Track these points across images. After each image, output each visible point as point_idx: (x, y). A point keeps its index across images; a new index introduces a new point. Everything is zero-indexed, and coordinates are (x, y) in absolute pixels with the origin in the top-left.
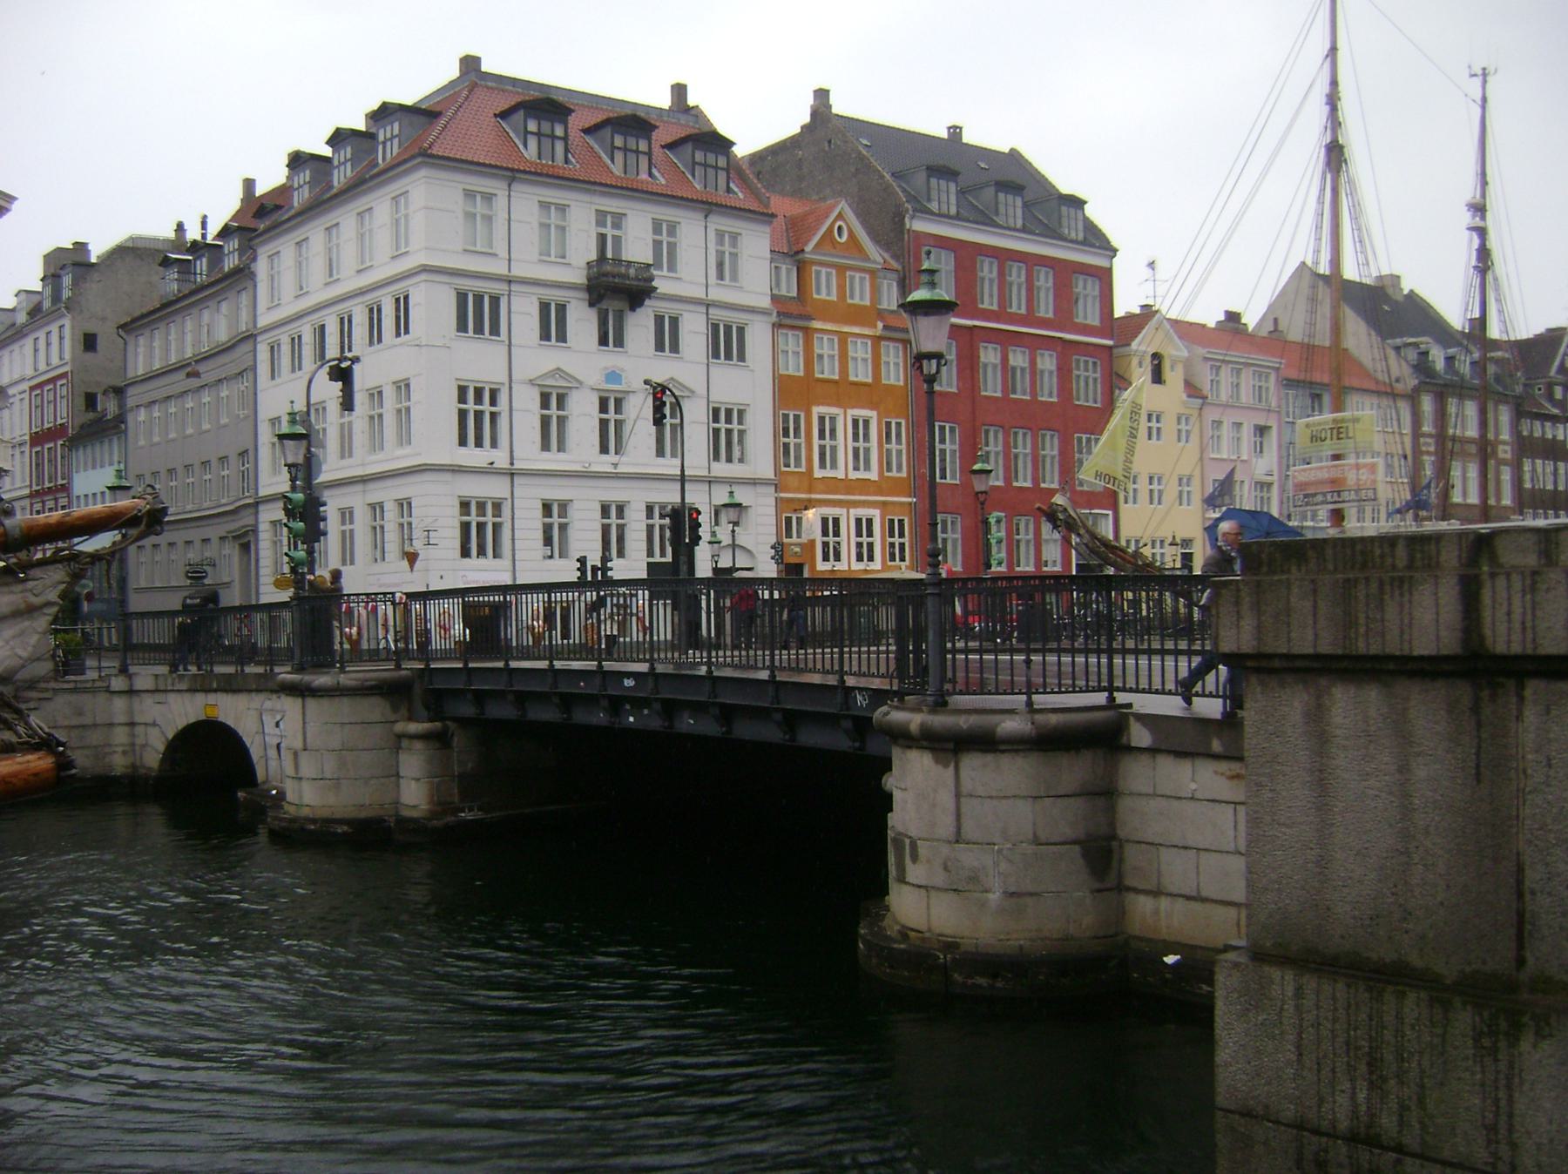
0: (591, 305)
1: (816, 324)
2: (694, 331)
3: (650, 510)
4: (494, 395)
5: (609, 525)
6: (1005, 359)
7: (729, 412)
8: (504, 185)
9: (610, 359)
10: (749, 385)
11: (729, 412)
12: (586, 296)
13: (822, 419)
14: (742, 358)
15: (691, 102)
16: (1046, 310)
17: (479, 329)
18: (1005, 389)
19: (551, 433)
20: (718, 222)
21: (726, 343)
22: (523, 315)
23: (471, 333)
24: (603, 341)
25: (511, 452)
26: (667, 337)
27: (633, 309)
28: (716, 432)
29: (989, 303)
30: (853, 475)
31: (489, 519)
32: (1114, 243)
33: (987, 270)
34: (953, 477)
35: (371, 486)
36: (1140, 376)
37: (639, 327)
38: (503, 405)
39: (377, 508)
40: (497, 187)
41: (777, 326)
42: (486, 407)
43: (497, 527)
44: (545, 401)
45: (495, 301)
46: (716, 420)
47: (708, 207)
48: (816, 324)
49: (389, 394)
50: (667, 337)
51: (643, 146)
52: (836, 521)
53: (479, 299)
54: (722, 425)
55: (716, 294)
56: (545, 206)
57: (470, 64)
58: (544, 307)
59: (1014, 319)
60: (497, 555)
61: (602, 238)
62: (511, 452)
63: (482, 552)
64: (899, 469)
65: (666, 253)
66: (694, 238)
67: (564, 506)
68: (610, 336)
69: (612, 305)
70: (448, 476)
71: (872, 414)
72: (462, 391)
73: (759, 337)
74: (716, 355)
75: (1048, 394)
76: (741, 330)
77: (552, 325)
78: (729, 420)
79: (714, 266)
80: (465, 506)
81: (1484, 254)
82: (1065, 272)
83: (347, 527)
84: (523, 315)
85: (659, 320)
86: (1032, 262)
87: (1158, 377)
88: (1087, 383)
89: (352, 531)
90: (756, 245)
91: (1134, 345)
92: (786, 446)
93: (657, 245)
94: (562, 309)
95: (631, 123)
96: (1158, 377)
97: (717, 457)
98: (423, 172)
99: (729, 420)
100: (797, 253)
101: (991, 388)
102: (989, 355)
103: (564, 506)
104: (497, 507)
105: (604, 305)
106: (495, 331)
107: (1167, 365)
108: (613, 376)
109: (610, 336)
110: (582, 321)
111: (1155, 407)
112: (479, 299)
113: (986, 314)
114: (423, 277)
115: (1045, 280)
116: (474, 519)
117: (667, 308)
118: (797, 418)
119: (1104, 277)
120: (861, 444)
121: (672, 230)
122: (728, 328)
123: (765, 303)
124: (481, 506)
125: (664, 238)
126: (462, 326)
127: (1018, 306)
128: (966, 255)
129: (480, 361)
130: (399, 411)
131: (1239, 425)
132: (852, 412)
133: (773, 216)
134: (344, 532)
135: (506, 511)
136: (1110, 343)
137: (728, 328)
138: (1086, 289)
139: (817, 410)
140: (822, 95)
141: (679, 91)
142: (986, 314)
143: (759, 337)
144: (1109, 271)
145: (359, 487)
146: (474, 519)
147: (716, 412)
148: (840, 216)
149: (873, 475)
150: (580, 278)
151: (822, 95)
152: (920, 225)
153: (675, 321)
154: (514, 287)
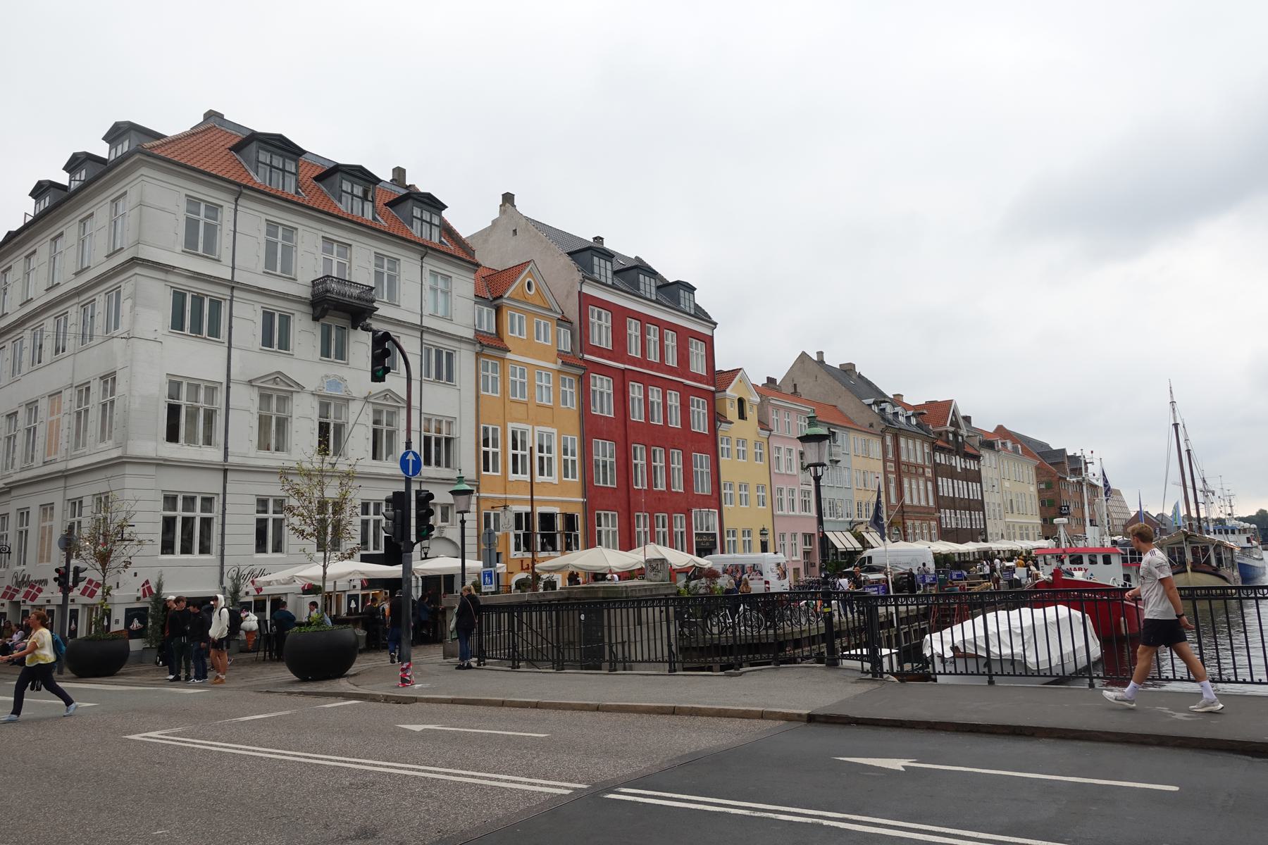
0: (315, 319)
3: (365, 507)
5: (266, 520)
6: (646, 396)
8: (231, 198)
9: (333, 369)
12: (310, 310)
13: (514, 434)
15: (408, 183)
16: (672, 361)
18: (646, 418)
19: (273, 431)
20: (431, 264)
22: (246, 320)
23: (187, 331)
24: (326, 352)
25: (226, 448)
26: (383, 355)
27: (355, 328)
29: (635, 352)
31: (198, 514)
32: (714, 319)
33: (633, 328)
34: (612, 483)
35: (72, 482)
39: (77, 504)
43: (206, 523)
45: (216, 304)
49: (96, 387)
53: (198, 300)
55: (428, 322)
58: (268, 317)
59: (651, 365)
60: (205, 549)
61: (328, 262)
62: (226, 448)
63: (187, 549)
64: (574, 476)
68: (333, 349)
69: (334, 321)
70: (151, 470)
71: (555, 431)
73: (465, 361)
75: (675, 422)
76: (450, 356)
77: (275, 334)
80: (170, 501)
82: (684, 336)
83: (47, 524)
84: (246, 320)
86: (662, 325)
87: (742, 416)
89: (51, 528)
91: (728, 391)
92: (486, 454)
93: (379, 275)
94: (286, 320)
96: (742, 416)
98: (144, 170)
100: (495, 299)
101: (637, 415)
102: (636, 391)
104: (208, 502)
105: (327, 320)
106: (214, 332)
107: (747, 406)
109: (333, 349)
110: (305, 334)
112: (198, 300)
113: (633, 361)
114: (137, 270)
115: (671, 340)
116: (179, 514)
119: (709, 342)
124: (189, 501)
126: (177, 324)
127: (653, 357)
128: (620, 316)
129: (198, 359)
130: (104, 405)
131: (790, 451)
132: (537, 428)
133: (478, 265)
134: (44, 528)
135: (217, 506)
136: (713, 388)
138: (697, 350)
140: (508, 198)
142: (633, 361)
143: (465, 361)
144: (712, 338)
145: (61, 483)
146: (179, 514)
150: (306, 293)
151: (508, 198)
154: (236, 293)
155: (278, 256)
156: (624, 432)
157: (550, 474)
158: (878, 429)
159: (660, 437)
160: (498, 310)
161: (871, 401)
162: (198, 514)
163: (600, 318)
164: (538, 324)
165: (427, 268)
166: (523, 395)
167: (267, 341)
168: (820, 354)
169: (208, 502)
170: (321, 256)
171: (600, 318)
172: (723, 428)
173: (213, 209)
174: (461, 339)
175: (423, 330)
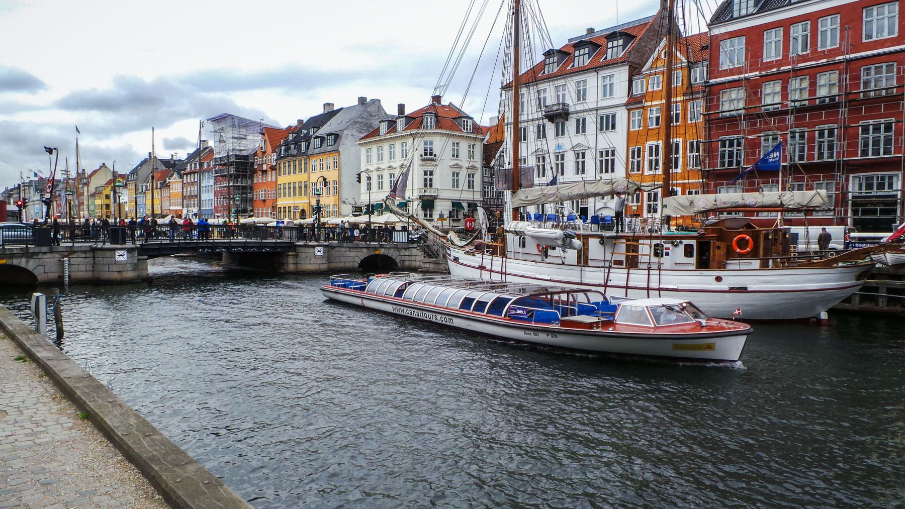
7: (607, 152)
10: (617, 140)
11: (607, 152)
21: (608, 123)
37: (571, 125)
46: (578, 158)
50: (581, 127)
54: (604, 158)
55: (600, 104)
61: (558, 96)
73: (622, 116)
78: (607, 155)
85: (578, 121)
99: (607, 155)
110: (550, 128)
113: (770, 65)
137: (608, 117)
143: (622, 116)
153: (584, 120)
165: (600, 76)
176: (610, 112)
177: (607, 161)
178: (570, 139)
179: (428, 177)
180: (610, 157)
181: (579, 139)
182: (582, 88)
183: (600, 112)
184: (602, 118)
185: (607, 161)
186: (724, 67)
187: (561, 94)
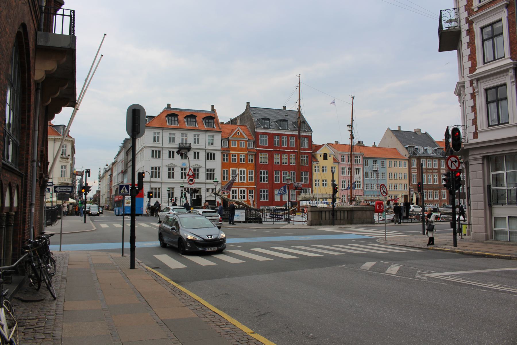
1: (231, 152)
2: (203, 155)
4: (159, 169)
10: (216, 165)
14: (214, 159)
17: (156, 157)
19: (171, 175)
20: (208, 134)
21: (210, 157)
22: (165, 154)
28: (207, 174)
30: (240, 182)
33: (276, 139)
36: (320, 159)
37: (191, 155)
38: (161, 171)
40: (160, 131)
41: (222, 153)
42: (157, 171)
44: (169, 169)
45: (159, 151)
47: (206, 131)
48: (231, 152)
50: (197, 156)
51: (194, 120)
52: (236, 191)
54: (209, 173)
56: (170, 134)
57: (169, 105)
58: (170, 152)
61: (182, 139)
65: (197, 141)
66: (203, 136)
67: (173, 189)
72: (152, 168)
74: (208, 159)
76: (214, 155)
77: (171, 155)
78: (210, 171)
79: (207, 142)
81: (352, 135)
84: (165, 154)
85: (195, 153)
88: (305, 161)
90: (218, 138)
92: (224, 176)
95: (191, 116)
97: (207, 179)
99: (210, 171)
103: (173, 189)
104: (159, 188)
106: (159, 157)
108: (184, 164)
111: (324, 165)
117: (197, 151)
118: (227, 171)
119: (310, 138)
120: (242, 175)
121: (198, 136)
122: (211, 154)
123: (220, 148)
124: (156, 189)
125: (196, 138)
128: (271, 136)
129: (156, 162)
132: (240, 169)
139: (231, 169)
140: (248, 103)
141: (213, 106)
143: (218, 156)
144: (311, 136)
147: (208, 171)
148: (238, 130)
149: (245, 181)
151: (248, 103)
152: (258, 130)
155: (172, 140)
156: (271, 167)
157: (244, 180)
158: (407, 157)
159: (283, 168)
160: (229, 141)
161: (407, 146)
162: (157, 191)
163: (263, 137)
164: (241, 143)
165: (207, 135)
166: (235, 161)
167: (170, 157)
168: (399, 127)
169: (159, 188)
170: (181, 138)
171: (263, 137)
172: (315, 164)
173: (159, 133)
174: (216, 150)
175: (206, 150)
176: (212, 152)
177: (211, 174)
178: (191, 162)
179: (63, 169)
180: (212, 173)
181: (196, 162)
182: (196, 138)
183: (208, 151)
184: (208, 154)
185: (211, 174)
186: (260, 145)
187: (184, 137)
